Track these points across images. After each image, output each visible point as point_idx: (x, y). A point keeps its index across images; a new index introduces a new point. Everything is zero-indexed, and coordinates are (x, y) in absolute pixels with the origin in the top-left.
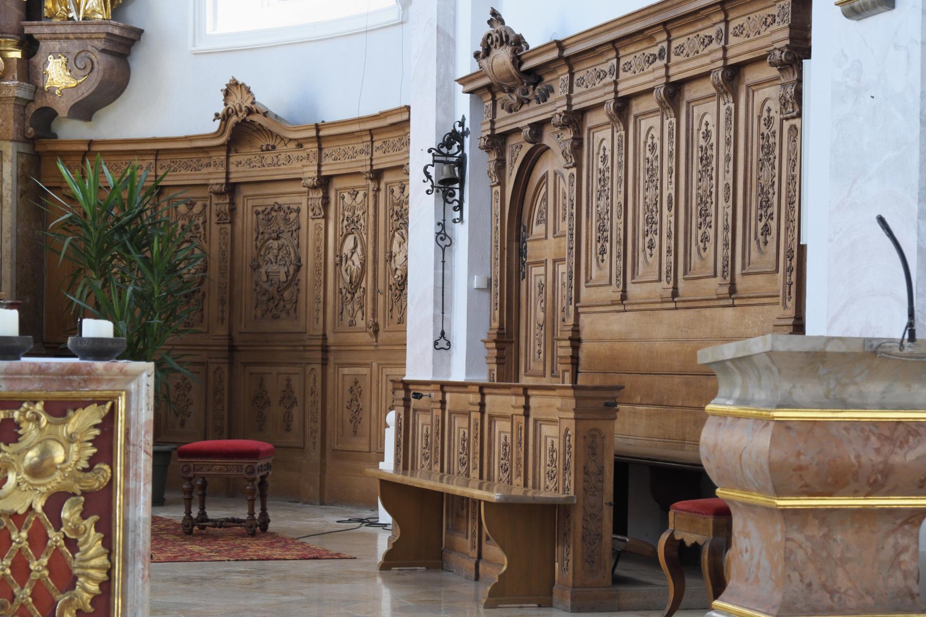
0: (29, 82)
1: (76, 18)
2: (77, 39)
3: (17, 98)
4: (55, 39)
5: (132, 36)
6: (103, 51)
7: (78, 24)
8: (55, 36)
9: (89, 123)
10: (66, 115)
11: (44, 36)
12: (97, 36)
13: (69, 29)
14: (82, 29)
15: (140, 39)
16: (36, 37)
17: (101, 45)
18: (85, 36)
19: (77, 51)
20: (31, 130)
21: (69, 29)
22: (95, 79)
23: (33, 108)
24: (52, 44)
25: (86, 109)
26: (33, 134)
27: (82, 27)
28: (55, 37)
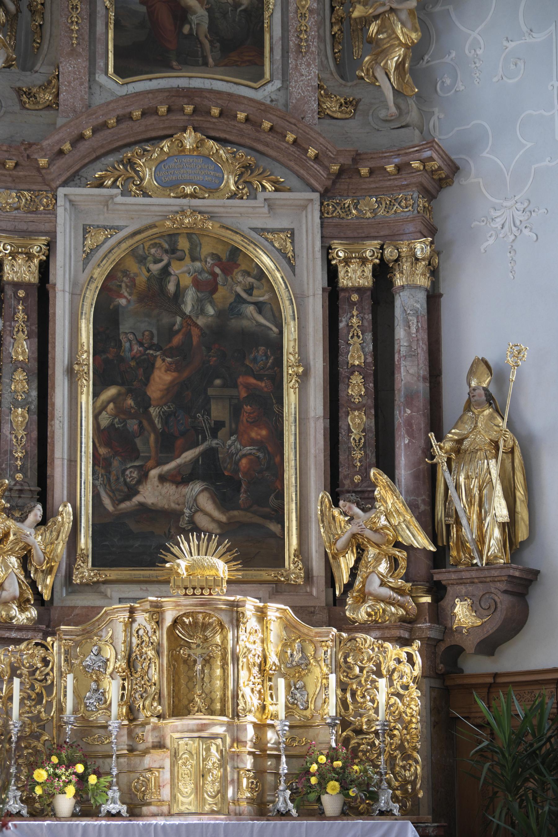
0: (438, 624)
1: (479, 564)
2: (481, 582)
3: (429, 638)
4: (461, 584)
5: (530, 577)
6: (505, 592)
7: (481, 569)
8: (461, 581)
9: (492, 658)
10: (473, 651)
11: (452, 582)
12: (499, 579)
13: (474, 574)
14: (486, 573)
15: (536, 579)
16: (444, 583)
17: (503, 586)
18: (488, 579)
19: (481, 594)
20: (441, 666)
21: (474, 574)
22: (499, 617)
23: (443, 647)
24: (458, 588)
25: (490, 645)
26: (443, 670)
27: (486, 572)
28: (461, 582)
